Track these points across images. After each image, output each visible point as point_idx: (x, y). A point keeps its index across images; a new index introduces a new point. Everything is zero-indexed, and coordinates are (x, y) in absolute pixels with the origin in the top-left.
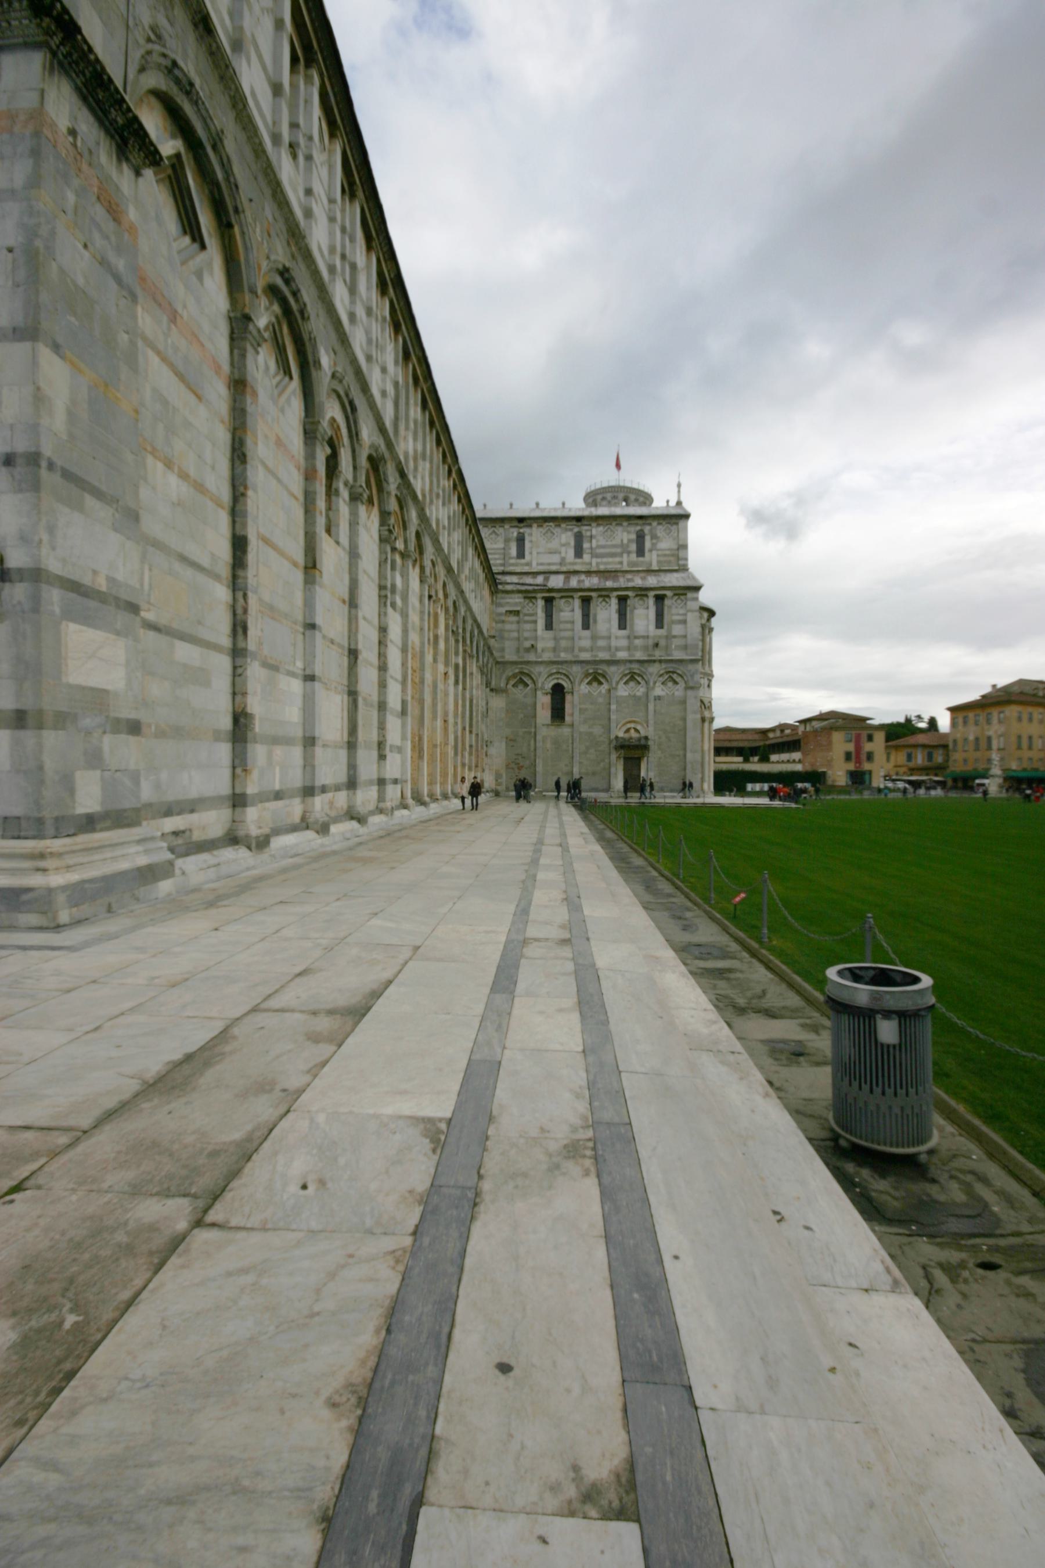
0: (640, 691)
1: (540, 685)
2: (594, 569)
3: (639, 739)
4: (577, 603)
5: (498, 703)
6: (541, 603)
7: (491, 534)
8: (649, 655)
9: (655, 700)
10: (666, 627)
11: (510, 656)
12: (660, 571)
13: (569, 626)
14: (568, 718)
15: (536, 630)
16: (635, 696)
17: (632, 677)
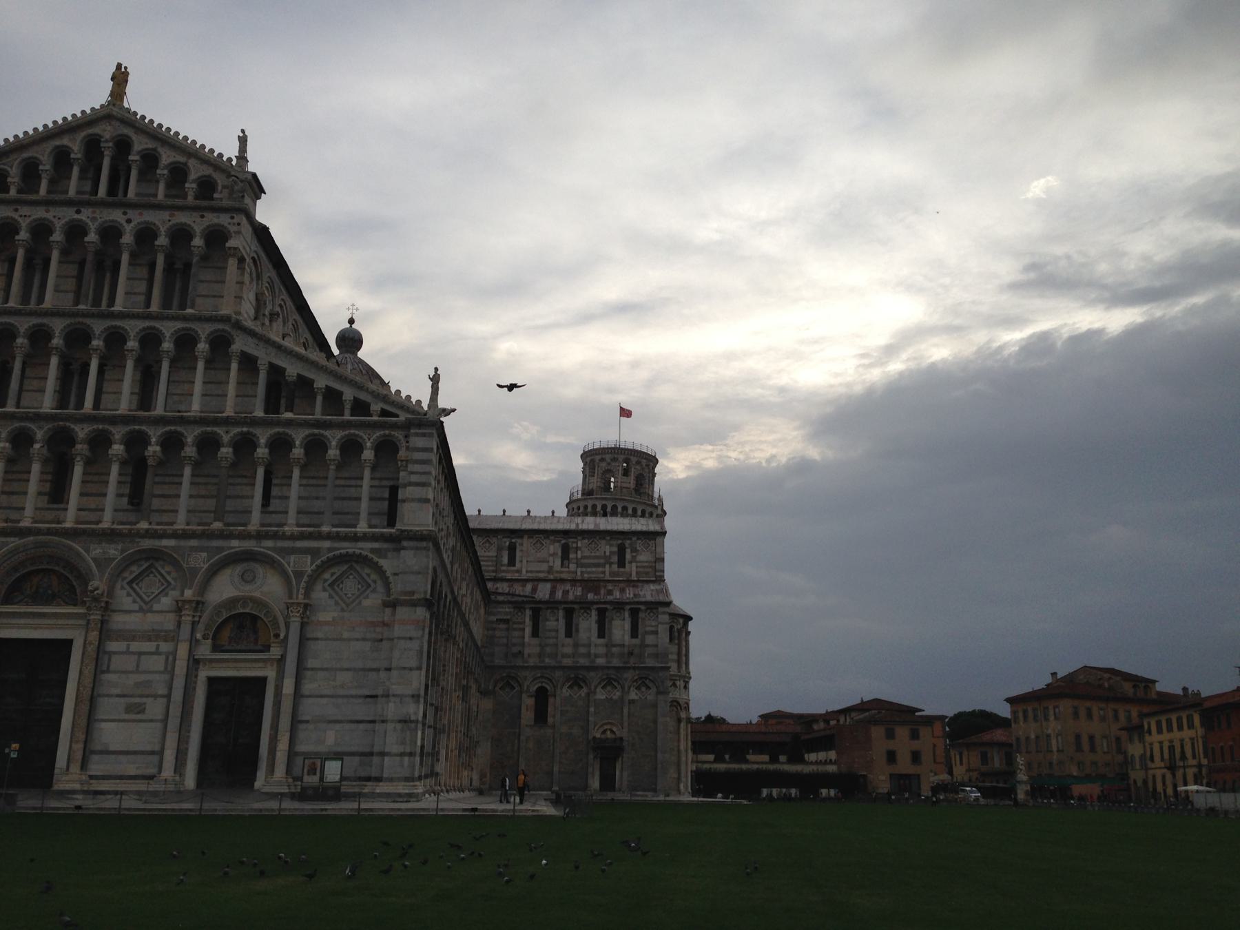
0: (617, 695)
1: (525, 688)
2: (579, 577)
3: (615, 740)
4: (561, 613)
5: (487, 704)
6: (528, 612)
7: (485, 543)
8: (624, 663)
9: (630, 703)
10: (640, 637)
11: (498, 661)
12: (638, 581)
13: (553, 634)
14: (550, 720)
15: (524, 638)
16: (611, 699)
17: (609, 682)
